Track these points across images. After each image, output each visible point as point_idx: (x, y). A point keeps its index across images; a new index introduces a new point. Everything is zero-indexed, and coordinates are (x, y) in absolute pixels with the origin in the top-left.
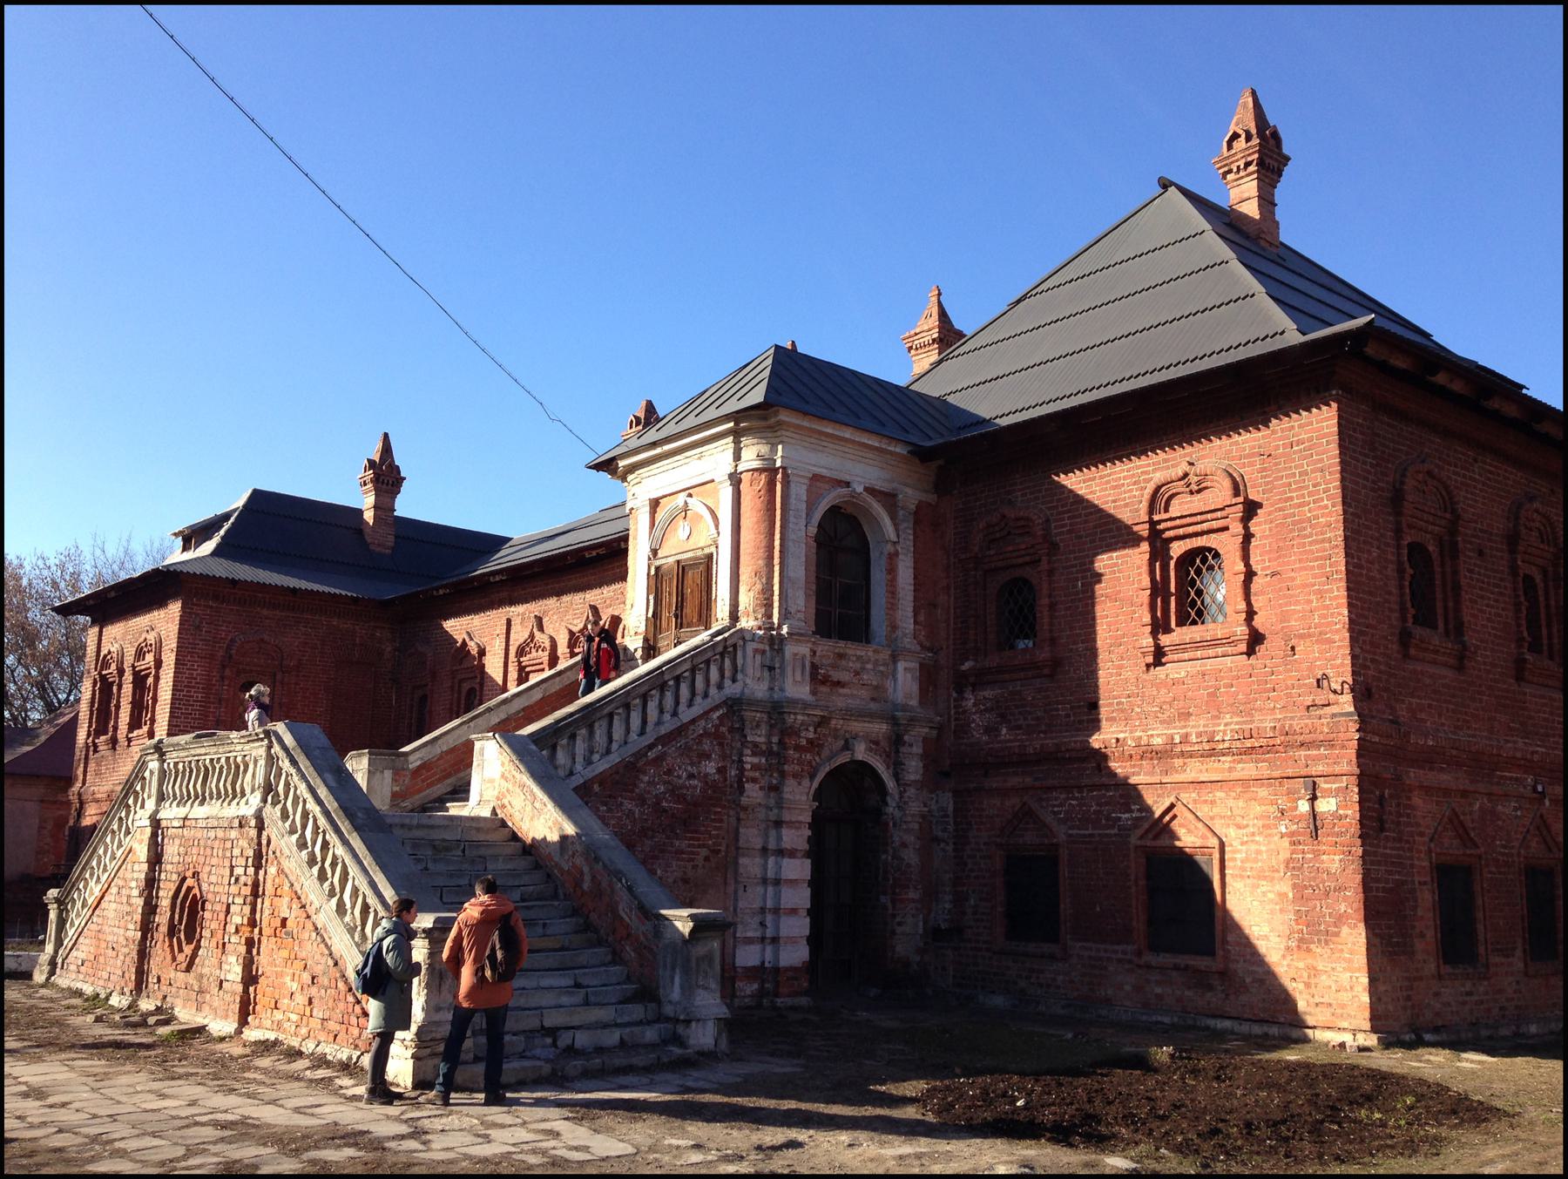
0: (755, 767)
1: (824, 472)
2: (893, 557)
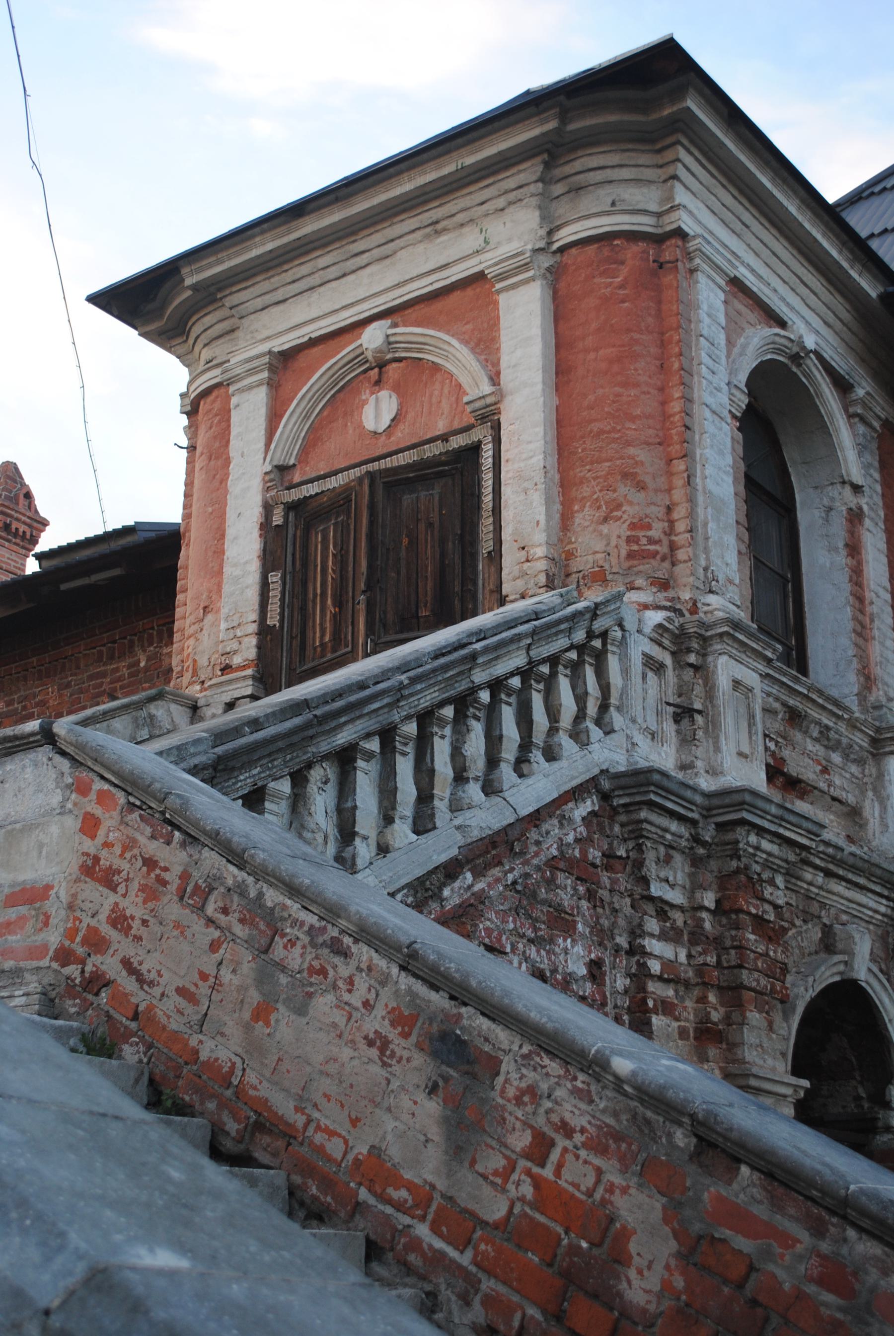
0: (669, 977)
1: (750, 280)
2: (855, 517)
